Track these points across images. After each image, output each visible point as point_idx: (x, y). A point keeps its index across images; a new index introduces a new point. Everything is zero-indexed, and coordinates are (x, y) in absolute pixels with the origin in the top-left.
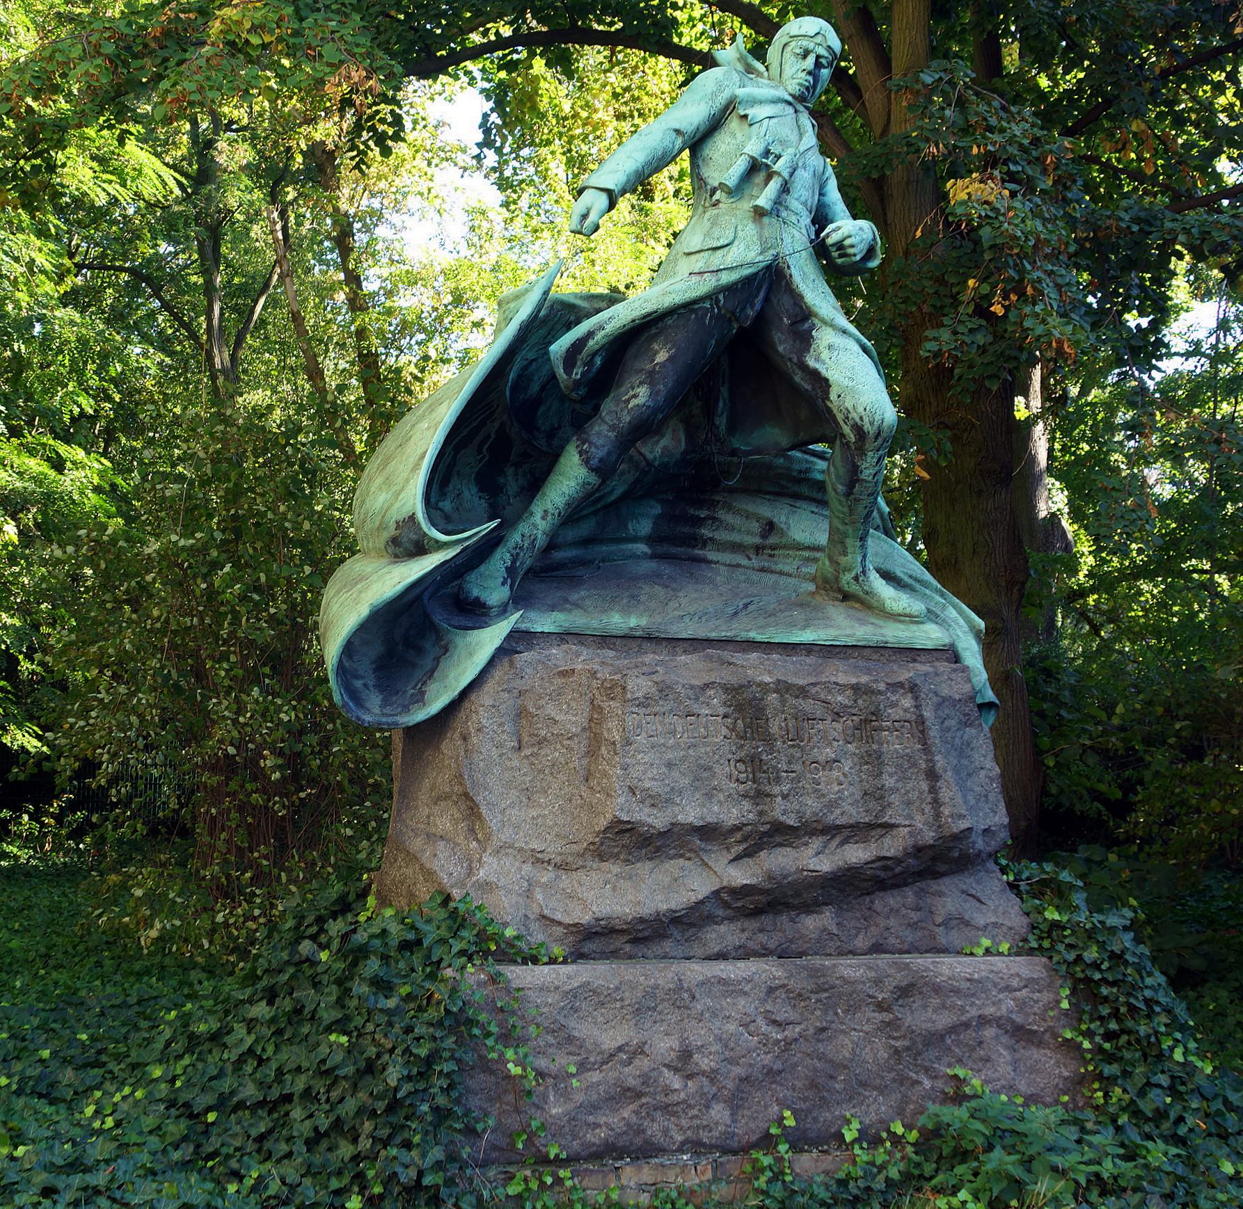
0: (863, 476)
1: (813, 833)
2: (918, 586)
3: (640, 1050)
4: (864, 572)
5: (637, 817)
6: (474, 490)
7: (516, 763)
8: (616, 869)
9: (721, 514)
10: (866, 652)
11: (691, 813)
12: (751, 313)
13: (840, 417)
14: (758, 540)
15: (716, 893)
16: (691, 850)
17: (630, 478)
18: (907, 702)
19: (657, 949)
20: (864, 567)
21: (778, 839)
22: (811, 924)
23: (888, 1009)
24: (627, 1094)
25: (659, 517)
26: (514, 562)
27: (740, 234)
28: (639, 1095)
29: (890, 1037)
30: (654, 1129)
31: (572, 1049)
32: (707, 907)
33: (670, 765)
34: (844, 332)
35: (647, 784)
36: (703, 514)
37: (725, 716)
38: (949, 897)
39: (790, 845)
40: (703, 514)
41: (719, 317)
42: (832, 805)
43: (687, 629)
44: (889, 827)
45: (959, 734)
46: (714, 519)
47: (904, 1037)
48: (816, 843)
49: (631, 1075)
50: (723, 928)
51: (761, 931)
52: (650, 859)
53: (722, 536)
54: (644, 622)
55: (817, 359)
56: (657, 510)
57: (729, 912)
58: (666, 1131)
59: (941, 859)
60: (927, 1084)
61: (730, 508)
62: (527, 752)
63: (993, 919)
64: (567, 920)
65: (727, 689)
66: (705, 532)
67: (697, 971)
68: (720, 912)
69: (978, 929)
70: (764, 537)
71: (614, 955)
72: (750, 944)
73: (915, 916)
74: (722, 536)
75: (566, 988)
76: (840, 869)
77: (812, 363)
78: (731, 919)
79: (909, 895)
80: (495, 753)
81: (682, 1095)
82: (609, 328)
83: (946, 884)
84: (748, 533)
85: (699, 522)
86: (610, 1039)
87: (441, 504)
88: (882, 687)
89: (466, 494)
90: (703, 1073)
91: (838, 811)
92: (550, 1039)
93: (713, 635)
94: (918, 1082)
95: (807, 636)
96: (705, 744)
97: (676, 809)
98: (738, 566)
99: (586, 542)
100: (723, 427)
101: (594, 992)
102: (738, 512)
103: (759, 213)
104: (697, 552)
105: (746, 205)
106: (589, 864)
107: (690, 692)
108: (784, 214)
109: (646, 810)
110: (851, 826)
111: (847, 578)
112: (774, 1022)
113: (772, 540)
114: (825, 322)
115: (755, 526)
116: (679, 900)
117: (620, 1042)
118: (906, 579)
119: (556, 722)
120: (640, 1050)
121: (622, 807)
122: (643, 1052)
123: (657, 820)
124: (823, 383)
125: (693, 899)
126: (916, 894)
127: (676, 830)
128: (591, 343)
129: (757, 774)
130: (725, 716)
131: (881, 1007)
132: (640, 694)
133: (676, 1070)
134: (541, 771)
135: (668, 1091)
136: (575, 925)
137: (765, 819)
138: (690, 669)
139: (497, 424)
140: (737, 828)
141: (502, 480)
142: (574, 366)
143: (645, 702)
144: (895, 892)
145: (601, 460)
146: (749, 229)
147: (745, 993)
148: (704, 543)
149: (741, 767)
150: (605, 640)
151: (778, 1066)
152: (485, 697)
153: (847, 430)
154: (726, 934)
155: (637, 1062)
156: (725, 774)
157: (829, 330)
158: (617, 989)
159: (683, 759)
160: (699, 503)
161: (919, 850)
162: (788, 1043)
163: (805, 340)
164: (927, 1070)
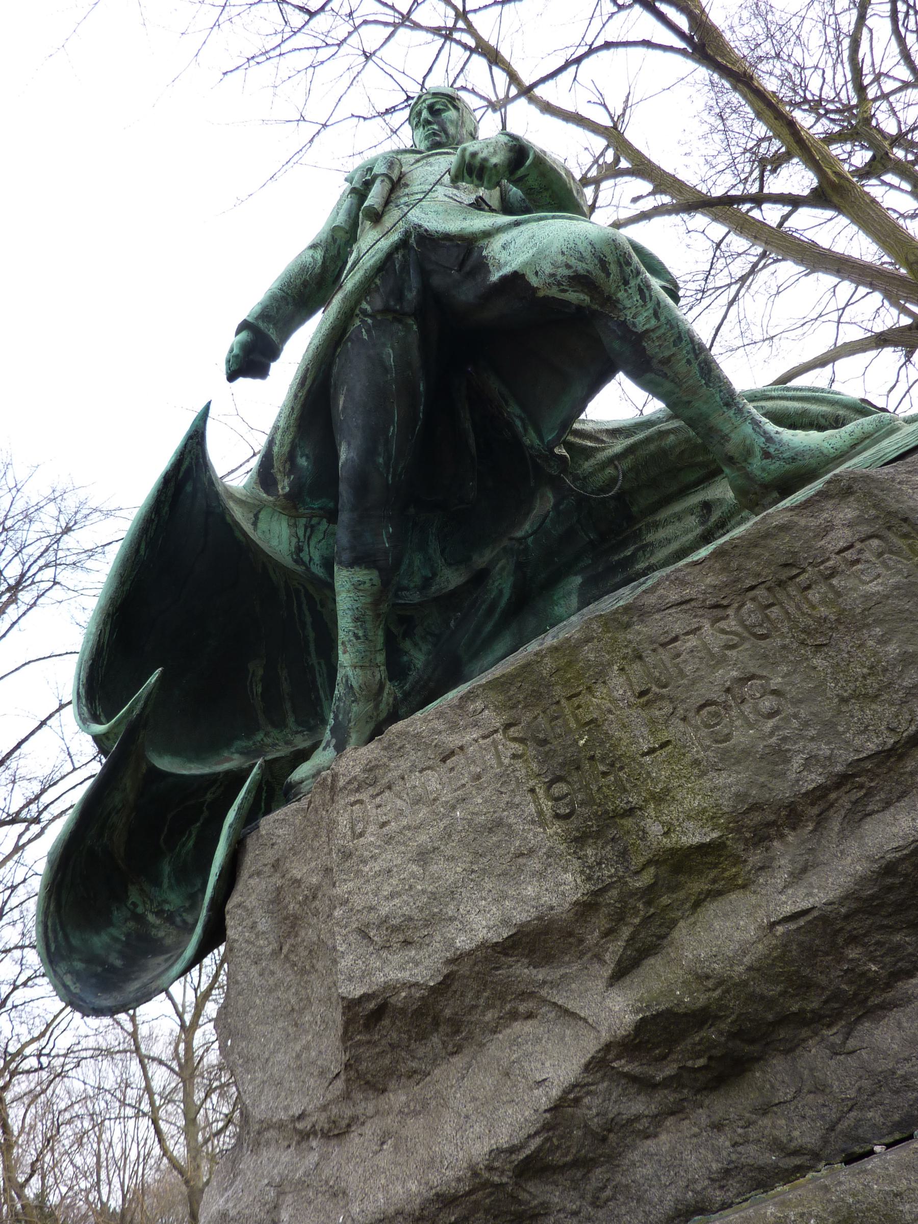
0: (640, 329)
1: (761, 837)
5: (380, 978)
8: (397, 1098)
11: (480, 922)
13: (554, 292)
14: (699, 530)
15: (597, 1065)
16: (524, 996)
18: (848, 512)
21: (698, 886)
25: (582, 585)
32: (592, 1108)
35: (384, 911)
37: (507, 726)
42: (778, 755)
48: (785, 853)
51: (765, 1110)
56: (578, 580)
57: (659, 1096)
61: (656, 525)
68: (639, 1106)
72: (752, 1154)
76: (863, 880)
78: (676, 1111)
84: (686, 532)
91: (797, 762)
96: (480, 789)
97: (451, 930)
102: (666, 522)
109: (396, 959)
111: (756, 464)
125: (544, 1103)
127: (464, 970)
128: (276, 449)
130: (507, 726)
137: (637, 861)
140: (586, 908)
141: (405, 658)
142: (275, 483)
149: (560, 788)
153: (574, 296)
156: (530, 820)
159: (447, 835)
160: (623, 544)
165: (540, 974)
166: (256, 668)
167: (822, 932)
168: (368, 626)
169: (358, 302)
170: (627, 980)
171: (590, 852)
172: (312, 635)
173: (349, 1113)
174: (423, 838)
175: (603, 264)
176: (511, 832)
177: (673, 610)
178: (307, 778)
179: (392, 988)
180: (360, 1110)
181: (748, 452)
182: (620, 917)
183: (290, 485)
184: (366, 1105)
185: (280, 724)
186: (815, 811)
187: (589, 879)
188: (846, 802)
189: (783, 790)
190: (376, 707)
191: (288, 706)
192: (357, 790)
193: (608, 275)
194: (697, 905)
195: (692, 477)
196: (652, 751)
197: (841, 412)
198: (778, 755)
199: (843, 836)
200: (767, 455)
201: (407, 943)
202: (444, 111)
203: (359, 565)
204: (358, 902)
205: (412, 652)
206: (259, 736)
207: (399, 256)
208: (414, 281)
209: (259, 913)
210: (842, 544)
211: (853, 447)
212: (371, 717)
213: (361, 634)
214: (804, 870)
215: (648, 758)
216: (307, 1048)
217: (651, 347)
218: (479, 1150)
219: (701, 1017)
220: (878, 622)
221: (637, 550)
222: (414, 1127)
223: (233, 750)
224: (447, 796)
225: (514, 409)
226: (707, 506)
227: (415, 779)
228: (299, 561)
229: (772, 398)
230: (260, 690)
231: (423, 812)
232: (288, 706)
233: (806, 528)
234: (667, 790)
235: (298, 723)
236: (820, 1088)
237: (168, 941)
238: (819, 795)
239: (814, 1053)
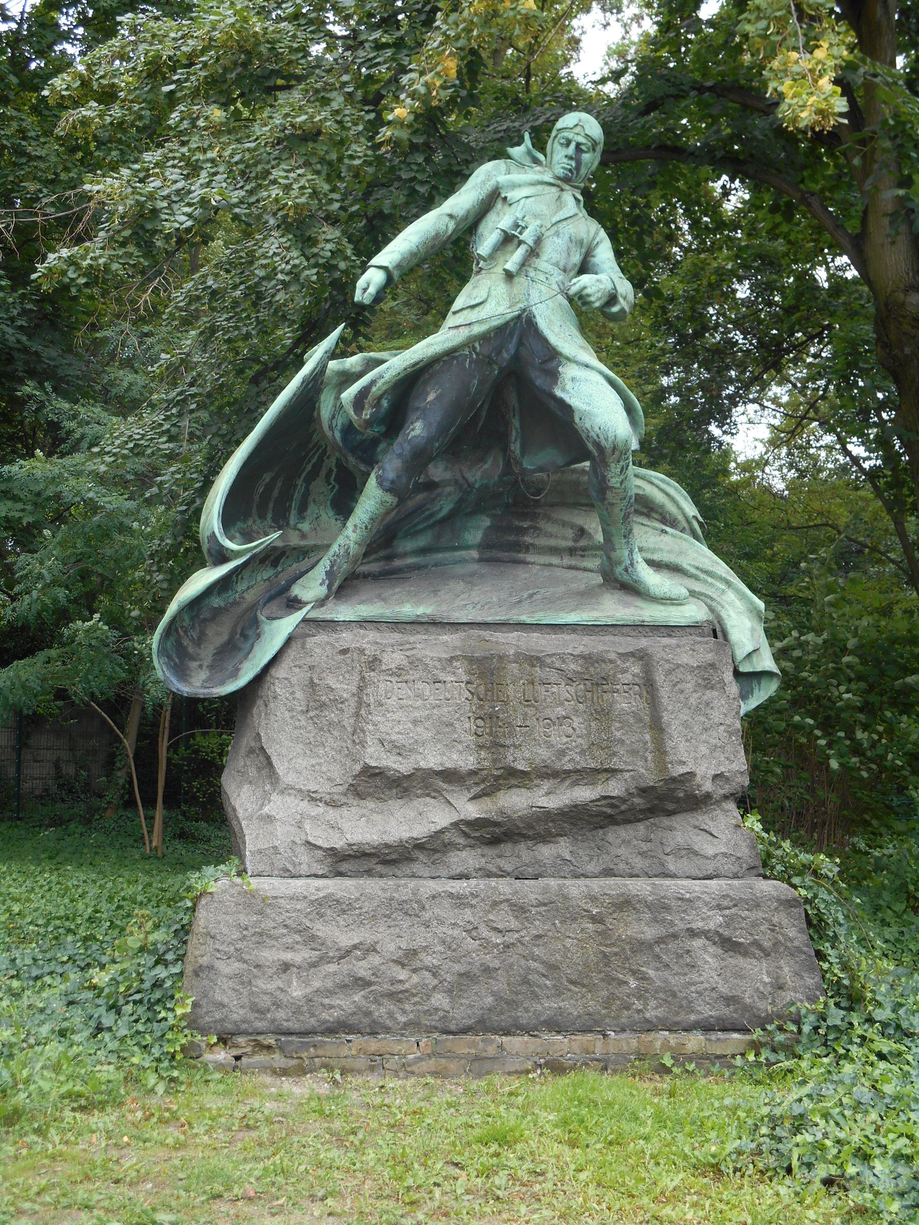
2: (702, 576)
3: (372, 949)
4: (632, 564)
6: (331, 513)
7: (303, 723)
8: (370, 804)
9: (542, 524)
10: (625, 630)
11: (432, 760)
12: (505, 355)
13: (584, 436)
14: (570, 544)
15: (455, 825)
17: (456, 497)
18: (636, 669)
19: (406, 869)
21: (513, 782)
22: (546, 852)
23: (601, 922)
24: (361, 983)
26: (332, 567)
27: (493, 293)
28: (369, 984)
29: (601, 944)
30: (380, 1012)
31: (314, 945)
32: (447, 837)
33: (415, 722)
34: (587, 366)
36: (525, 525)
38: (682, 831)
39: (524, 786)
40: (525, 525)
41: (477, 362)
42: (562, 753)
44: (613, 772)
45: (696, 695)
46: (535, 528)
47: (613, 945)
48: (546, 785)
49: (362, 969)
50: (464, 854)
53: (542, 541)
54: (429, 611)
55: (563, 390)
56: (487, 522)
58: (391, 1015)
59: (669, 799)
60: (633, 984)
61: (549, 519)
62: (311, 714)
63: (723, 850)
64: (326, 845)
65: (471, 660)
66: (528, 539)
67: (430, 887)
68: (461, 841)
69: (707, 858)
70: (575, 541)
71: (369, 873)
72: (491, 867)
73: (645, 847)
74: (542, 541)
75: (313, 898)
77: (559, 393)
79: (641, 827)
80: (287, 714)
81: (407, 986)
82: (387, 377)
83: (677, 821)
84: (564, 538)
85: (522, 531)
86: (346, 940)
87: (300, 526)
88: (613, 656)
89: (324, 517)
90: (427, 969)
91: (567, 758)
92: (297, 938)
93: (489, 619)
94: (626, 983)
95: (572, 618)
97: (419, 757)
98: (550, 565)
99: (423, 551)
100: (518, 452)
101: (338, 901)
102: (555, 522)
103: (509, 276)
104: (521, 556)
105: (499, 270)
106: (350, 801)
107: (437, 664)
108: (532, 274)
109: (393, 758)
110: (578, 771)
111: (619, 570)
112: (496, 929)
113: (582, 543)
114: (568, 359)
115: (570, 533)
116: (420, 831)
117: (356, 941)
118: (693, 571)
119: (332, 690)
120: (372, 949)
121: (375, 756)
122: (375, 950)
123: (401, 766)
124: (568, 409)
126: (647, 828)
128: (374, 389)
129: (493, 728)
131: (594, 919)
132: (393, 666)
133: (403, 966)
134: (321, 729)
135: (394, 981)
136: (332, 849)
138: (434, 647)
139: (333, 460)
140: (473, 773)
142: (362, 408)
143: (398, 672)
144: (628, 827)
145: (393, 482)
146: (500, 288)
147: (472, 906)
148: (527, 548)
149: (480, 723)
150: (397, 625)
151: (496, 964)
152: (280, 672)
153: (590, 446)
154: (467, 858)
155: (370, 958)
156: (465, 729)
157: (574, 366)
158: (358, 899)
159: (428, 717)
160: (524, 516)
161: (644, 791)
162: (507, 946)
163: (554, 376)
164: (634, 973)
165: (445, 786)
166: (267, 477)
167: (547, 815)
172: (309, 468)
173: (344, 800)
174: (417, 714)
175: (615, 448)
176: (455, 731)
179: (389, 769)
180: (350, 801)
181: (620, 563)
182: (483, 781)
184: (352, 800)
185: (262, 517)
189: (558, 766)
191: (271, 506)
195: (584, 501)
197: (680, 517)
200: (626, 570)
204: (382, 728)
206: (250, 522)
208: (512, 347)
209: (297, 688)
216: (320, 764)
217: (609, 495)
218: (405, 835)
219: (496, 824)
221: (531, 527)
222: (375, 817)
224: (432, 700)
225: (516, 423)
226: (582, 532)
227: (420, 685)
228: (331, 428)
231: (419, 703)
232: (271, 506)
235: (274, 520)
236: (518, 857)
237: (191, 650)
239: (522, 846)
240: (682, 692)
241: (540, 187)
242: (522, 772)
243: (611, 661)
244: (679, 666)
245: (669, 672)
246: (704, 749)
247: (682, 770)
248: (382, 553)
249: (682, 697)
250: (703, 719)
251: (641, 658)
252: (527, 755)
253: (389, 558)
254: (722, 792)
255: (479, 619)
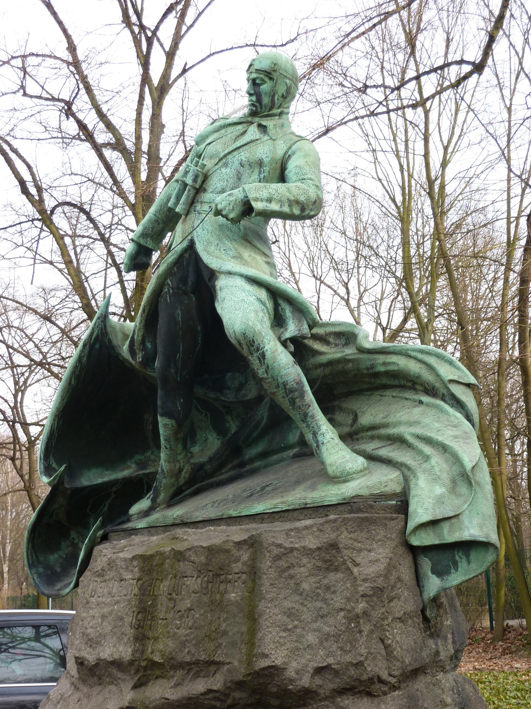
6: (215, 435)
20: (317, 442)
43: (200, 515)
45: (312, 579)
52: (100, 685)
76: (183, 698)
89: (211, 439)
95: (259, 508)
128: (136, 337)
141: (228, 425)
159: (110, 613)
165: (120, 675)
168: (172, 443)
169: (165, 279)
170: (137, 689)
171: (137, 645)
177: (190, 564)
178: (135, 514)
183: (142, 357)
186: (188, 668)
187: (133, 654)
188: (195, 670)
190: (177, 480)
192: (98, 576)
193: (243, 349)
194: (157, 678)
195: (365, 386)
196: (163, 619)
198: (183, 644)
199: (190, 681)
201: (91, 646)
202: (262, 84)
203: (166, 416)
205: (231, 423)
206: (148, 453)
207: (187, 255)
210: (237, 571)
211: (334, 478)
212: (174, 485)
213: (168, 447)
214: (179, 685)
215: (160, 622)
220: (227, 612)
223: (133, 461)
229: (410, 356)
230: (151, 428)
233: (233, 555)
234: (158, 638)
238: (189, 664)
240: (292, 577)
241: (223, 131)
242: (160, 664)
243: (227, 551)
244: (292, 550)
245: (277, 558)
246: (311, 638)
247: (264, 663)
248: (236, 462)
249: (292, 582)
250: (319, 604)
251: (252, 546)
252: (161, 647)
253: (242, 465)
254: (331, 686)
255: (213, 516)
